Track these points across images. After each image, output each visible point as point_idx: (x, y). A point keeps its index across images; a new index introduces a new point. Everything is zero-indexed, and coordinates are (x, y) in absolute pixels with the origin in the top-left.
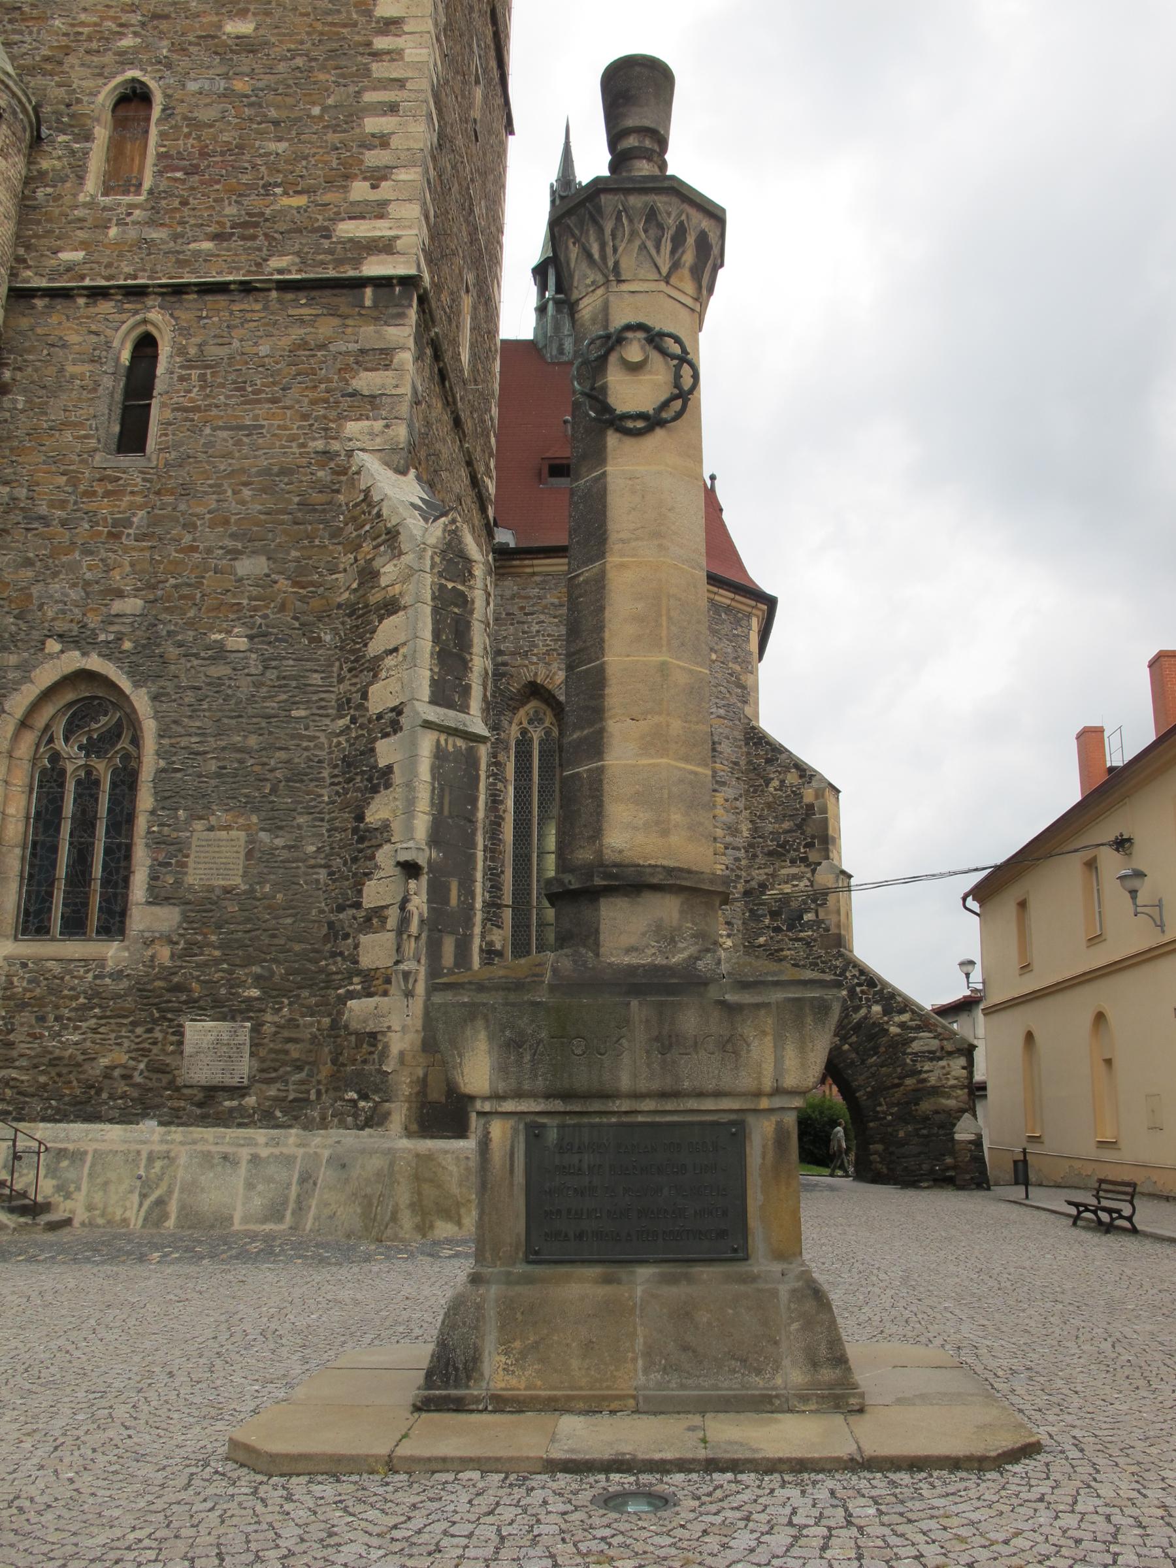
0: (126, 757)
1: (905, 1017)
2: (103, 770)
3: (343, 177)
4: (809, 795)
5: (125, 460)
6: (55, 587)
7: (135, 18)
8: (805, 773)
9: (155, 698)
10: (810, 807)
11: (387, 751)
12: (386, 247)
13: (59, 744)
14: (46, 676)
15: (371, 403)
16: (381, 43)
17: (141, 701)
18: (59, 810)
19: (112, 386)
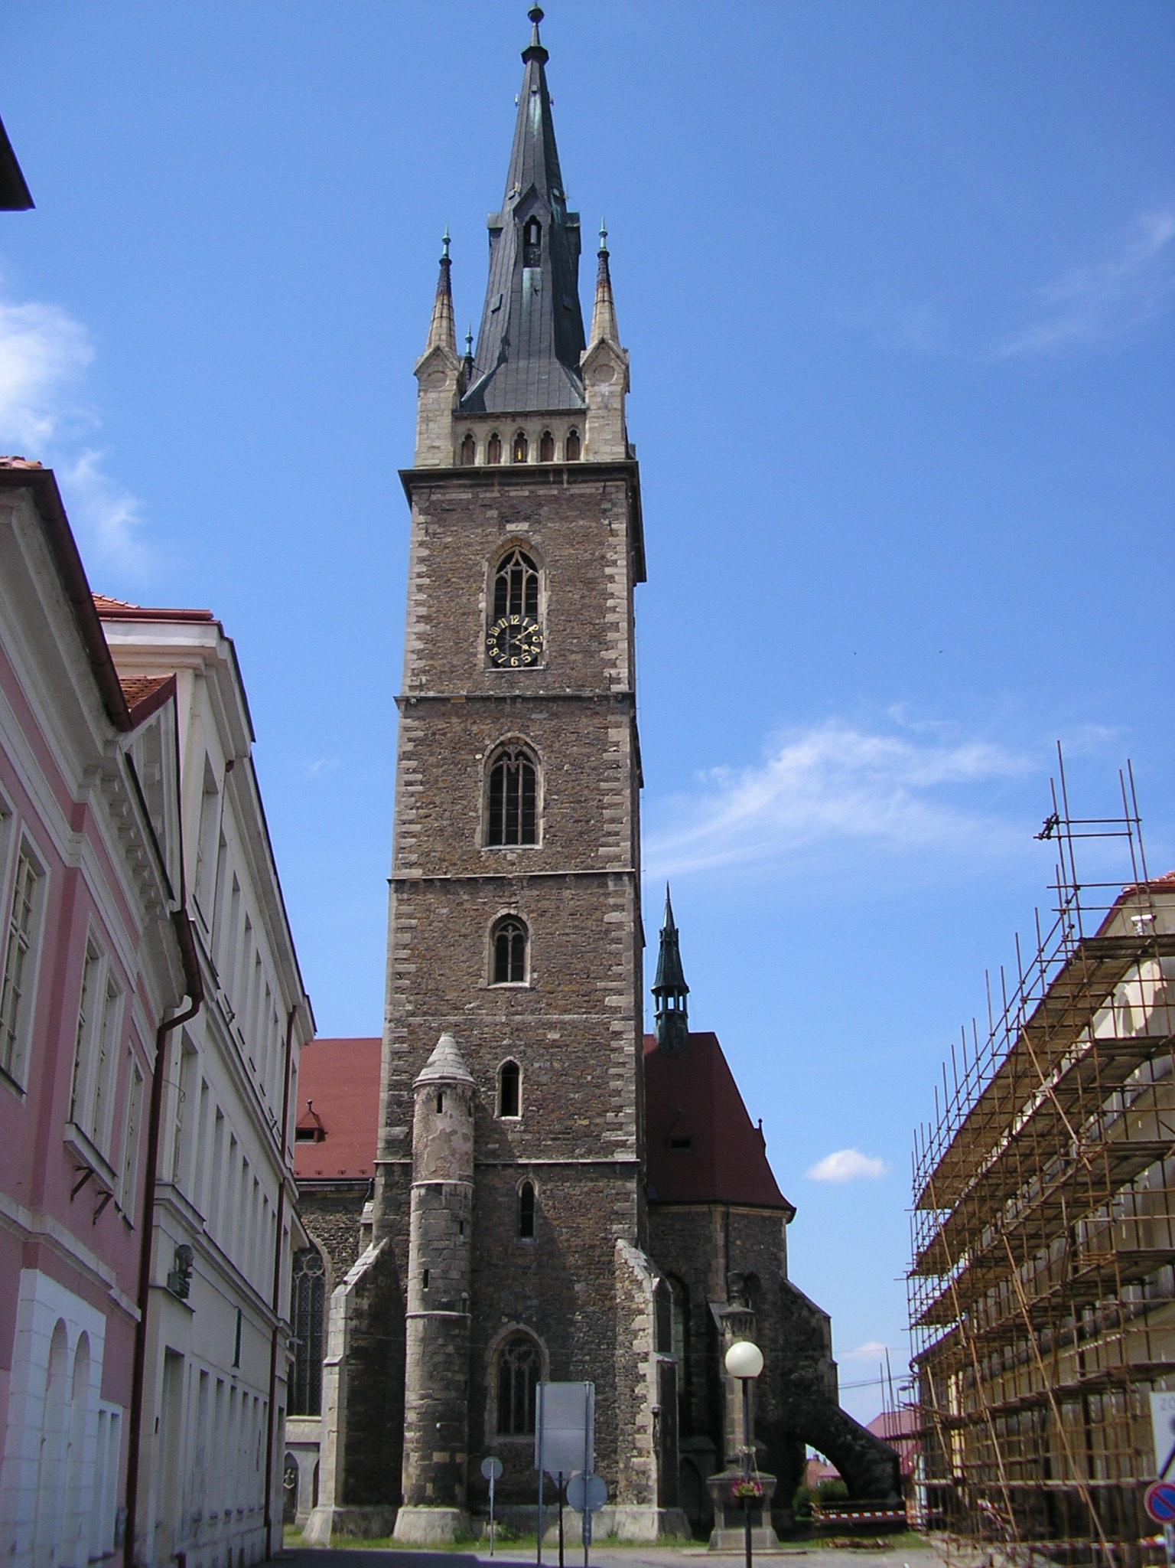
0: (534, 1362)
1: (862, 1442)
2: (526, 1367)
3: (602, 1114)
4: (814, 1322)
5: (527, 1240)
6: (503, 1295)
7: (507, 1030)
8: (813, 1310)
9: (547, 1341)
10: (814, 1329)
11: (643, 1368)
12: (623, 1144)
13: (508, 1357)
14: (503, 1332)
15: (620, 1216)
16: (614, 1044)
17: (542, 1341)
18: (509, 1384)
19: (517, 1206)
